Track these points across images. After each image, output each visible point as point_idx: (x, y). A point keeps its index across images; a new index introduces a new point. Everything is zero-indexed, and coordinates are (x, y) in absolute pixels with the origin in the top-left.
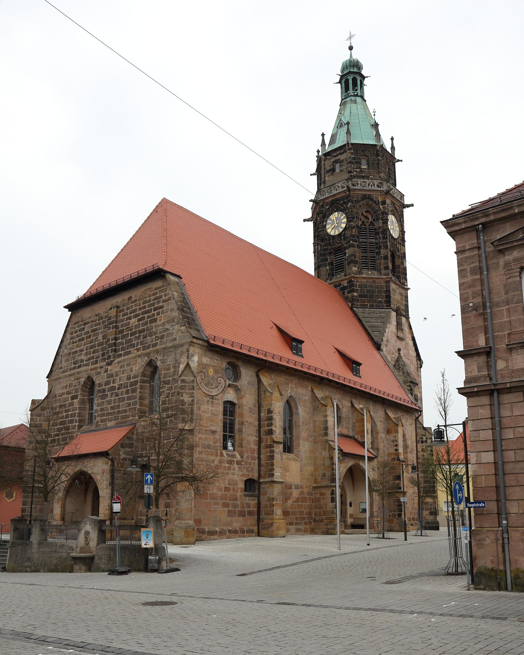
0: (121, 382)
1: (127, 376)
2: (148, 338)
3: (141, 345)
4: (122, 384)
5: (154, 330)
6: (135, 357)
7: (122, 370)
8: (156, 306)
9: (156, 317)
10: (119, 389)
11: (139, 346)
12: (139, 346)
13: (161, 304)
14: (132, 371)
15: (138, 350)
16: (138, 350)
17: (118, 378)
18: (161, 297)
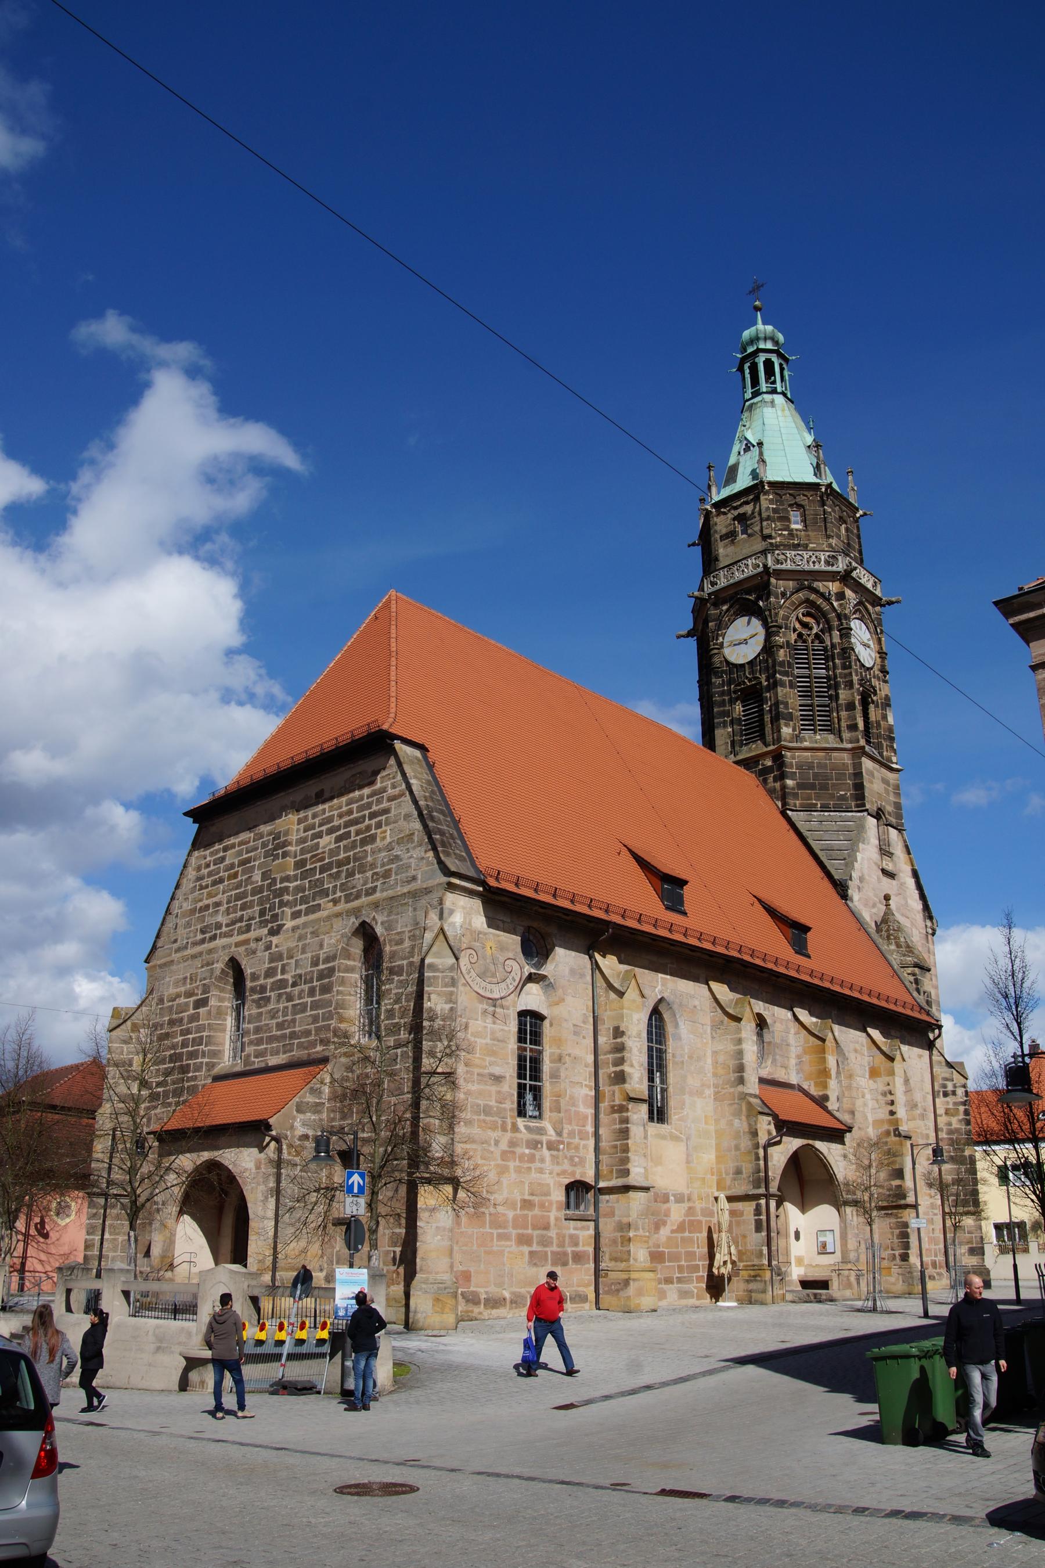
0: (299, 971)
1: (312, 958)
2: (357, 876)
3: (342, 891)
4: (300, 976)
5: (369, 859)
6: (329, 918)
7: (300, 944)
8: (374, 808)
9: (373, 831)
10: (294, 985)
11: (339, 894)
12: (339, 894)
13: (385, 805)
14: (321, 946)
15: (335, 902)
16: (335, 902)
17: (293, 961)
18: (384, 790)
